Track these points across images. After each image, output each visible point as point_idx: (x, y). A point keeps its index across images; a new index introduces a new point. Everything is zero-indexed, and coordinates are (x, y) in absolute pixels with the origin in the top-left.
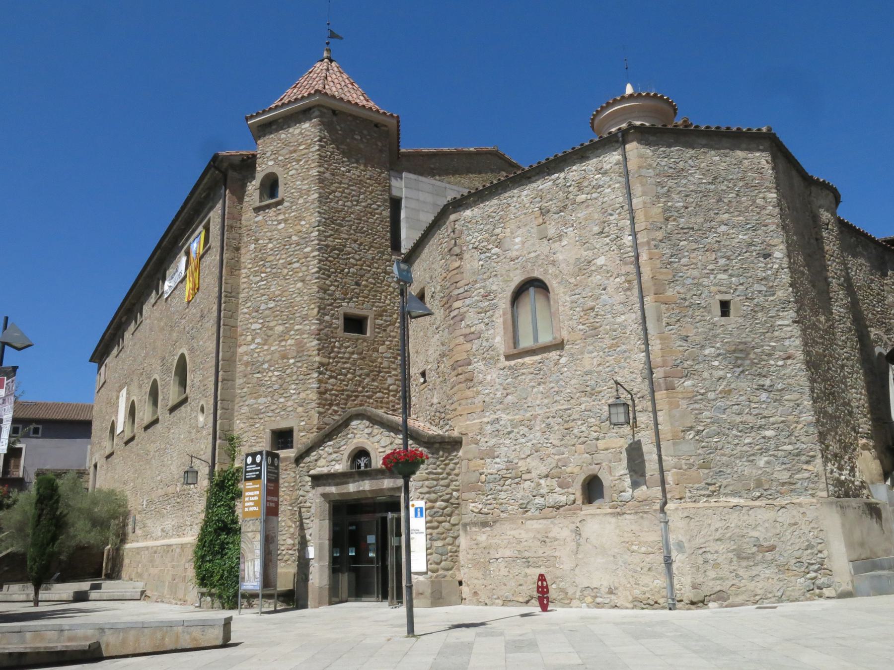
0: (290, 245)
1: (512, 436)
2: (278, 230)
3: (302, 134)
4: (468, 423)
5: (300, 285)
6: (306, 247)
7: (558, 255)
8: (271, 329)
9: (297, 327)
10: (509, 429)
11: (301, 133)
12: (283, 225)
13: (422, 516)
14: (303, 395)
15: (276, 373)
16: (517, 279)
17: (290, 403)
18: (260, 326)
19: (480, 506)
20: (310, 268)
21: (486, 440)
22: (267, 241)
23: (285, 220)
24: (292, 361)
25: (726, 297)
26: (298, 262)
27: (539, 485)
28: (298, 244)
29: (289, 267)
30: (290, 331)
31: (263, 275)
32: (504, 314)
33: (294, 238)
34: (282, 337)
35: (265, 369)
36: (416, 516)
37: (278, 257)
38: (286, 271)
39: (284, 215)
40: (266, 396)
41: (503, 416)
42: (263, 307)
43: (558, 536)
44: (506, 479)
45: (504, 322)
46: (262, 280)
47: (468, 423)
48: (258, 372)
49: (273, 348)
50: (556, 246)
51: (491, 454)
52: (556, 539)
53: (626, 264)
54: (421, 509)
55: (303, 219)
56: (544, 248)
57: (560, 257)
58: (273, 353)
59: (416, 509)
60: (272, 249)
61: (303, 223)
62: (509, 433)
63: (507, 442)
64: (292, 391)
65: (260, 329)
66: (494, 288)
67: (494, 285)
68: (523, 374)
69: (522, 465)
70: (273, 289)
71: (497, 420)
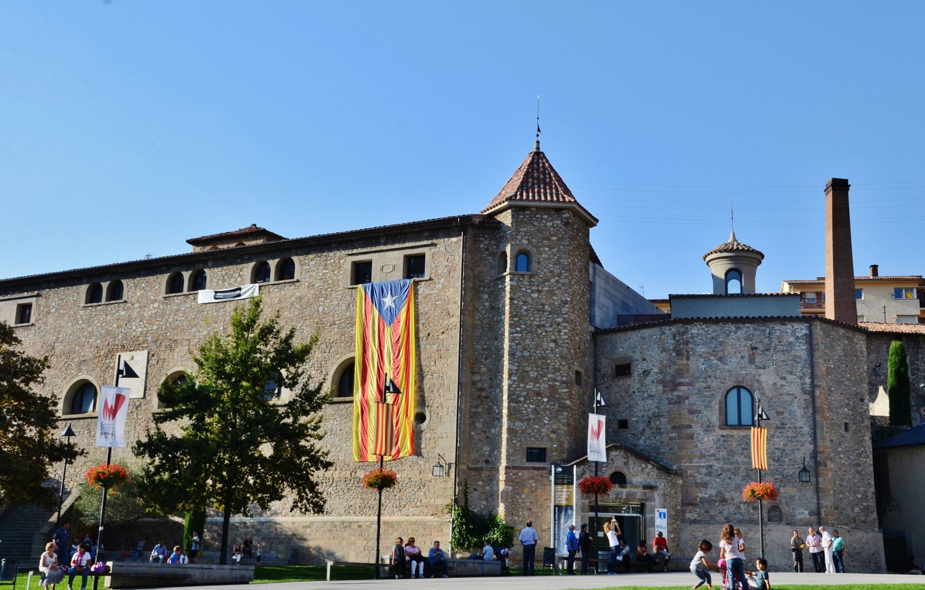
0: (544, 311)
1: (721, 476)
2: (531, 297)
3: (554, 228)
4: (688, 464)
5: (552, 345)
6: (558, 317)
7: (761, 377)
8: (527, 372)
9: (549, 376)
10: (720, 472)
11: (553, 227)
12: (535, 295)
13: (664, 517)
14: (554, 426)
15: (531, 406)
16: (730, 384)
17: (544, 430)
18: (516, 368)
19: (696, 516)
20: (561, 334)
21: (701, 476)
22: (522, 303)
23: (539, 291)
24: (545, 400)
25: (847, 421)
26: (551, 326)
27: (739, 507)
28: (550, 313)
29: (542, 328)
30: (544, 377)
31: (518, 329)
32: (720, 402)
33: (547, 307)
34: (536, 380)
35: (521, 402)
36: (660, 516)
37: (532, 319)
38: (540, 331)
39: (538, 286)
40: (522, 421)
41: (716, 464)
42: (518, 354)
43: (754, 537)
44: (717, 501)
45: (720, 408)
46: (517, 332)
47: (688, 464)
48: (516, 403)
49: (528, 387)
50: (761, 371)
51: (705, 485)
52: (752, 539)
53: (806, 394)
54: (664, 514)
55: (555, 295)
56: (751, 369)
57: (763, 378)
58: (528, 390)
59: (660, 514)
60: (526, 311)
61: (555, 298)
62: (719, 475)
63: (718, 480)
64: (545, 421)
65: (516, 370)
66: (713, 385)
67: (714, 384)
68: (732, 441)
69: (727, 496)
70: (527, 342)
71: (711, 466)
